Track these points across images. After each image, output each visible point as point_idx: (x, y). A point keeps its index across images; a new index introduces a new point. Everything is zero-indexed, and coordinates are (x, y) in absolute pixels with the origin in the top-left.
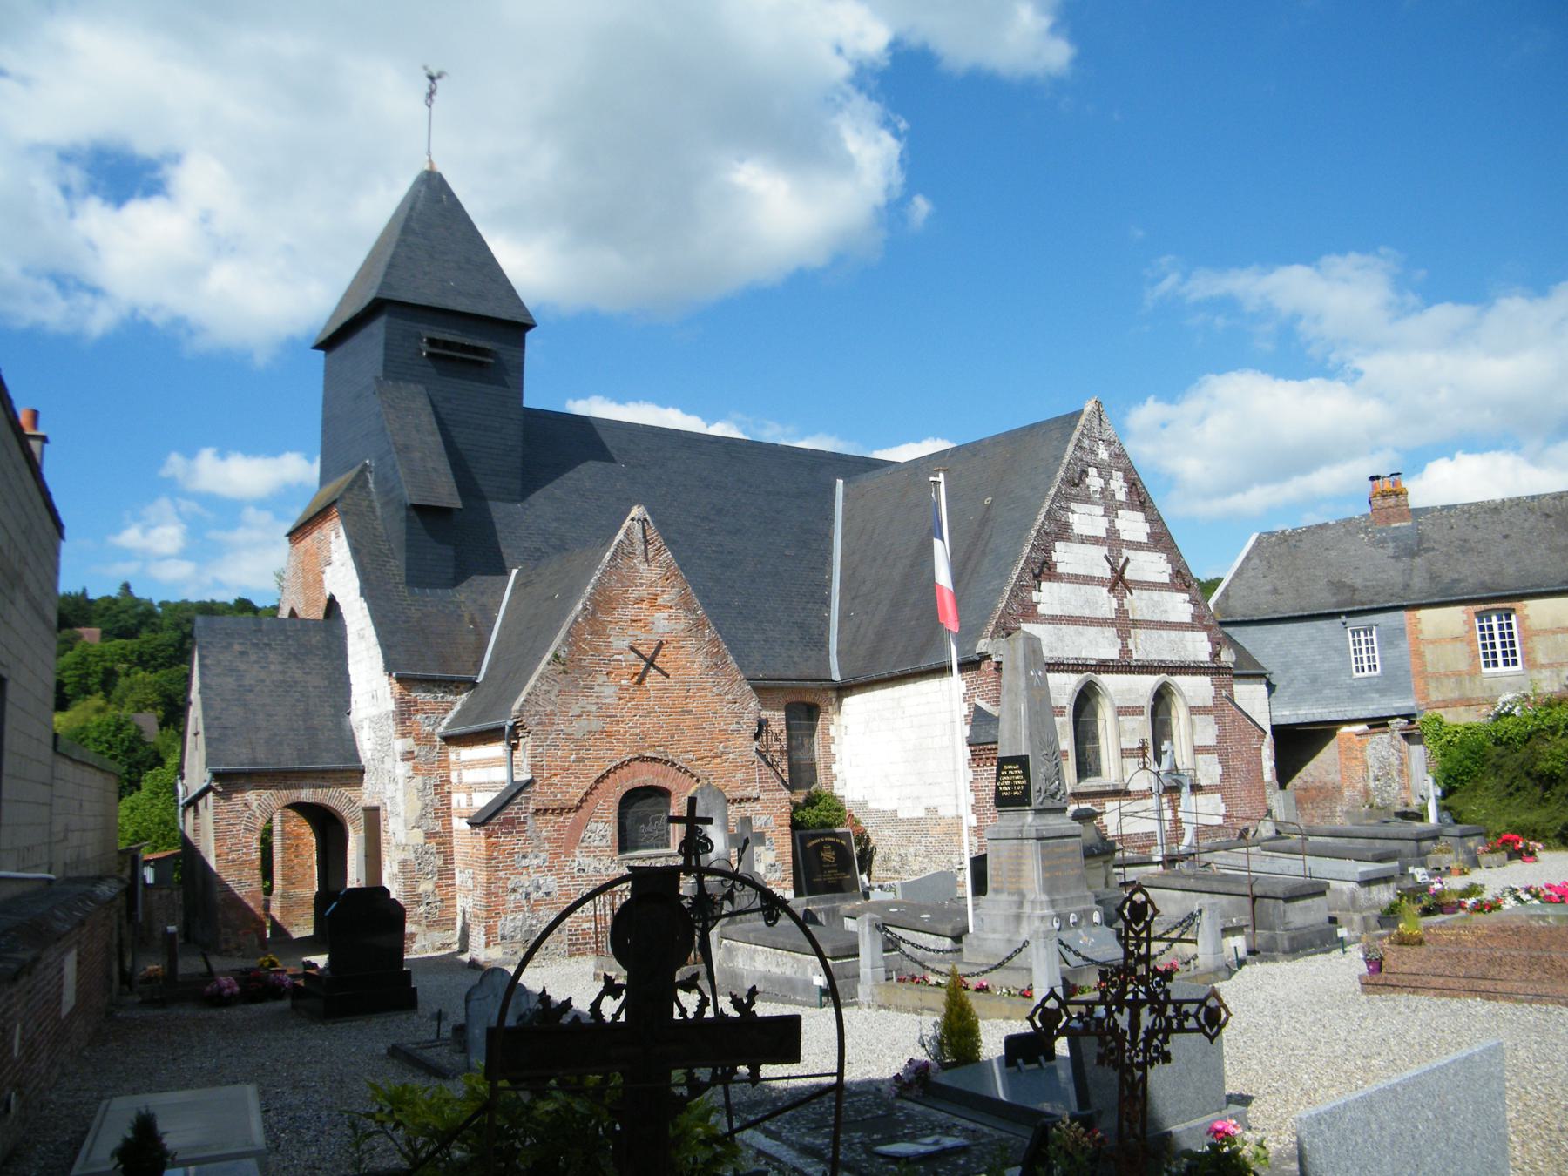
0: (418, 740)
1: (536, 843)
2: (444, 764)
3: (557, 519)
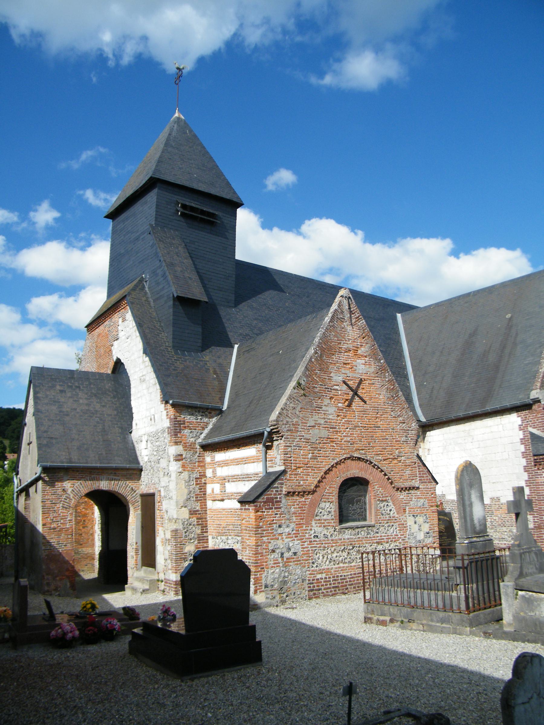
0: (185, 447)
1: (287, 516)
2: (202, 464)
3: (256, 319)
